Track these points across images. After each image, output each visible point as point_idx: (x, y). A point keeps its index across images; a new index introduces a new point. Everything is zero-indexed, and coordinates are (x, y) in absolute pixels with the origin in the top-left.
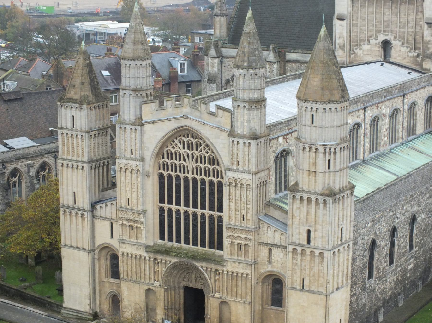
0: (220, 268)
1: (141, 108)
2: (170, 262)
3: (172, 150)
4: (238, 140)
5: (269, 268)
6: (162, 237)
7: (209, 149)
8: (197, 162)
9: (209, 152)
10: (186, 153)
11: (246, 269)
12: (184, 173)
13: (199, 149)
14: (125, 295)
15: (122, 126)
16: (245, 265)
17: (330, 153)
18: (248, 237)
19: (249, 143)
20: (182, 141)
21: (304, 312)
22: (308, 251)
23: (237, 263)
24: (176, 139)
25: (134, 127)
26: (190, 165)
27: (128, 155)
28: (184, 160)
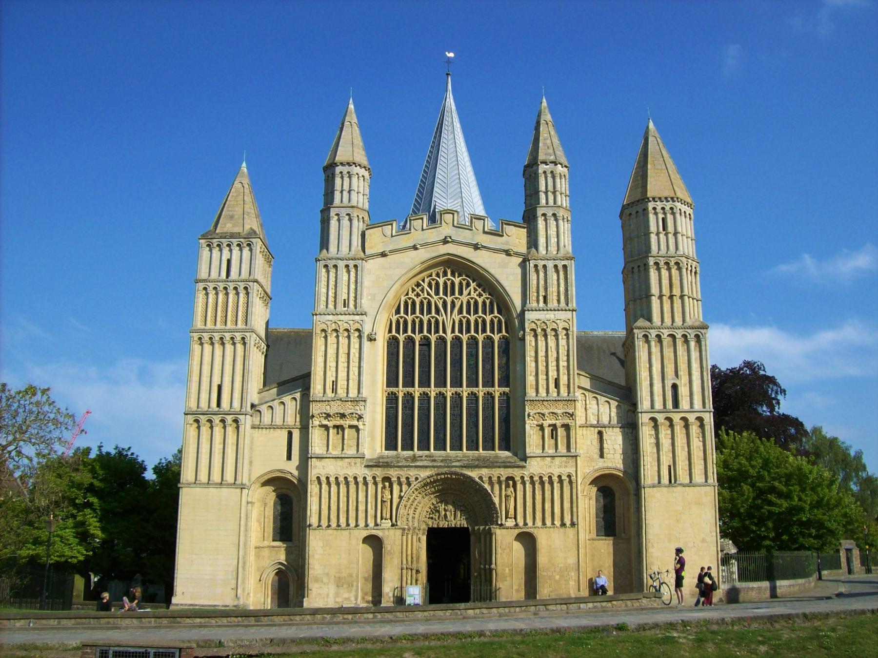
0: (517, 473)
1: (363, 235)
2: (417, 479)
3: (415, 298)
4: (543, 263)
5: (601, 463)
6: (391, 444)
7: (484, 291)
8: (460, 311)
9: (484, 294)
10: (441, 301)
11: (565, 467)
12: (437, 331)
13: (465, 292)
14: (316, 556)
15: (328, 262)
16: (565, 459)
17: (691, 275)
18: (570, 411)
19: (565, 267)
20: (433, 283)
21: (678, 521)
22: (676, 418)
23: (549, 459)
24: (423, 281)
25: (351, 263)
26: (450, 319)
27: (340, 308)
28: (438, 311)
